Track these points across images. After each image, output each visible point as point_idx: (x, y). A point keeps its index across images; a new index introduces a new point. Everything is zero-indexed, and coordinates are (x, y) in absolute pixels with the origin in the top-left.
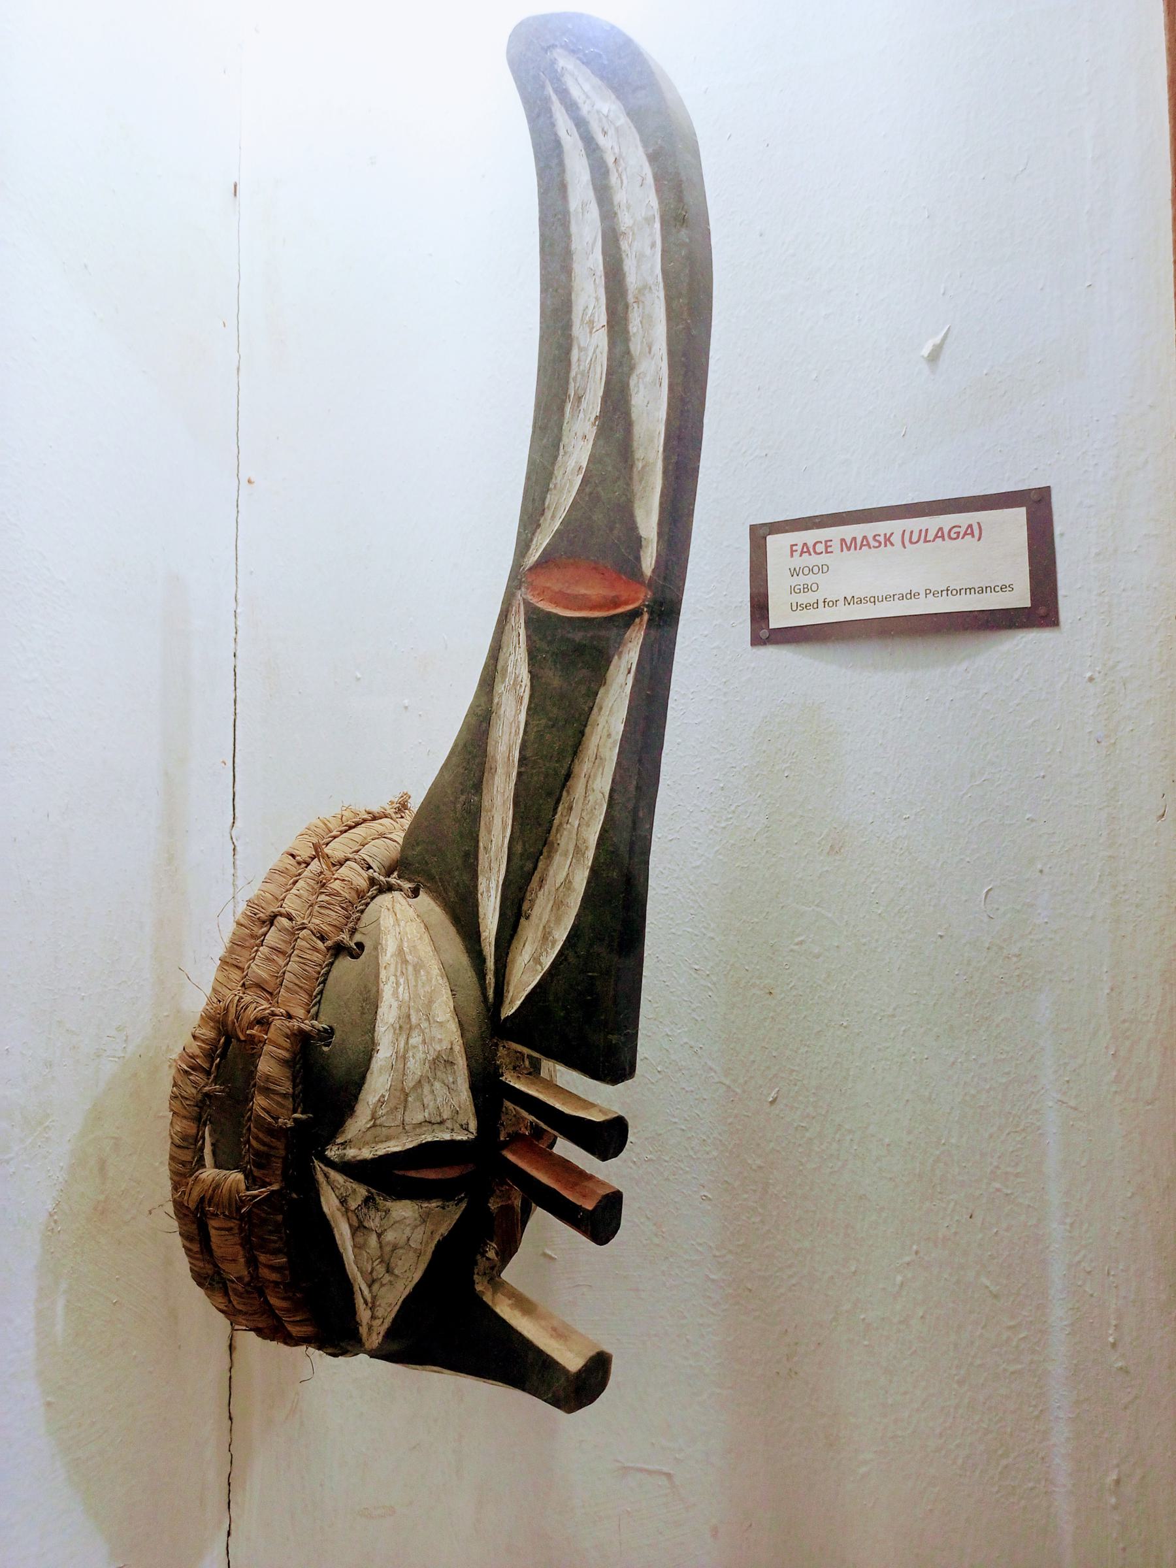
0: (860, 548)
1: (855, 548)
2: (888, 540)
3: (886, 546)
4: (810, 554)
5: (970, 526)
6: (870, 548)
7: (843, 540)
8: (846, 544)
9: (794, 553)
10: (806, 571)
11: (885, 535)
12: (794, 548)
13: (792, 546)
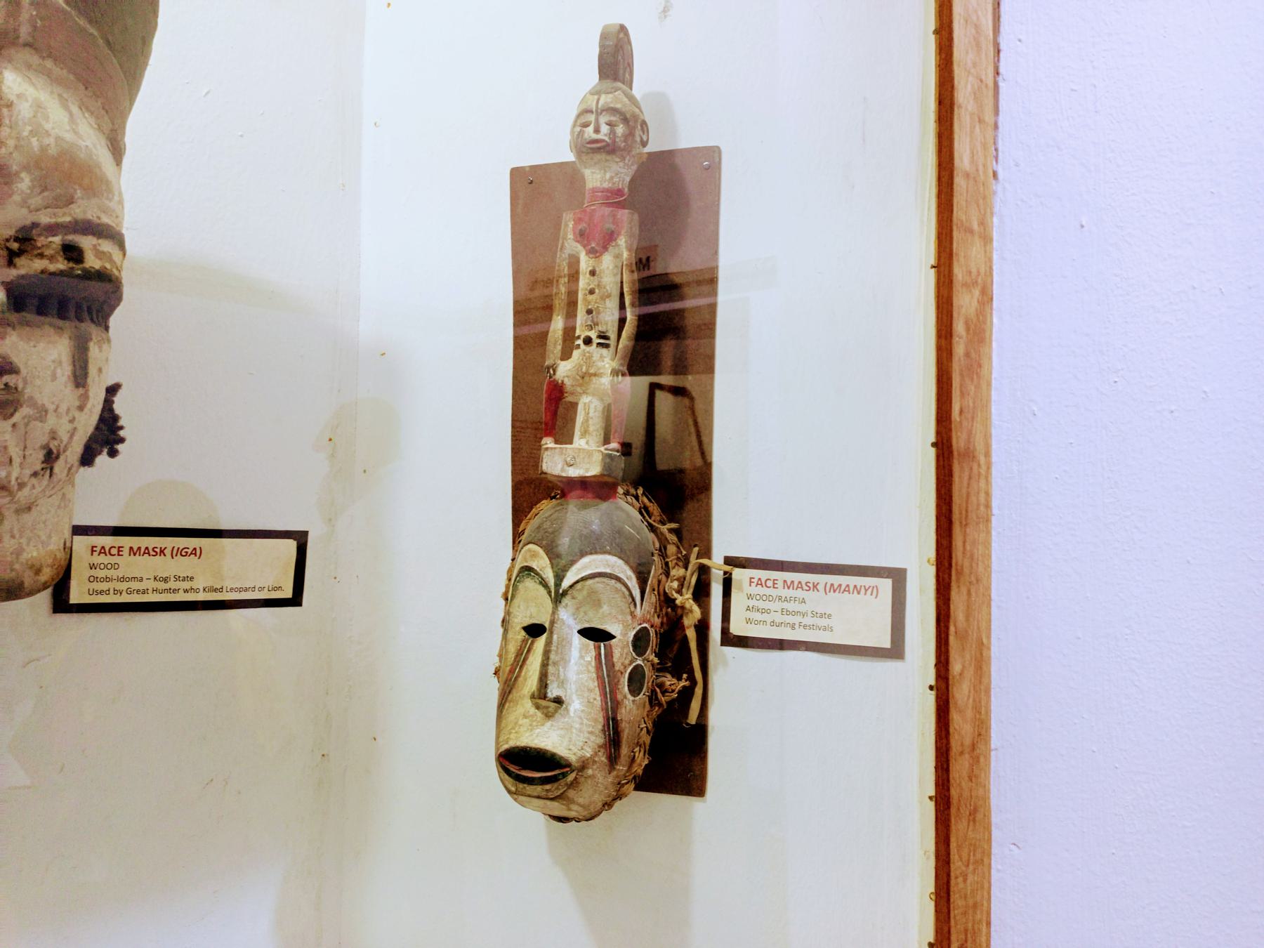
2: (162, 552)
4: (106, 555)
5: (195, 549)
7: (131, 548)
9: (94, 553)
10: (102, 566)
11: (161, 548)
12: (95, 549)
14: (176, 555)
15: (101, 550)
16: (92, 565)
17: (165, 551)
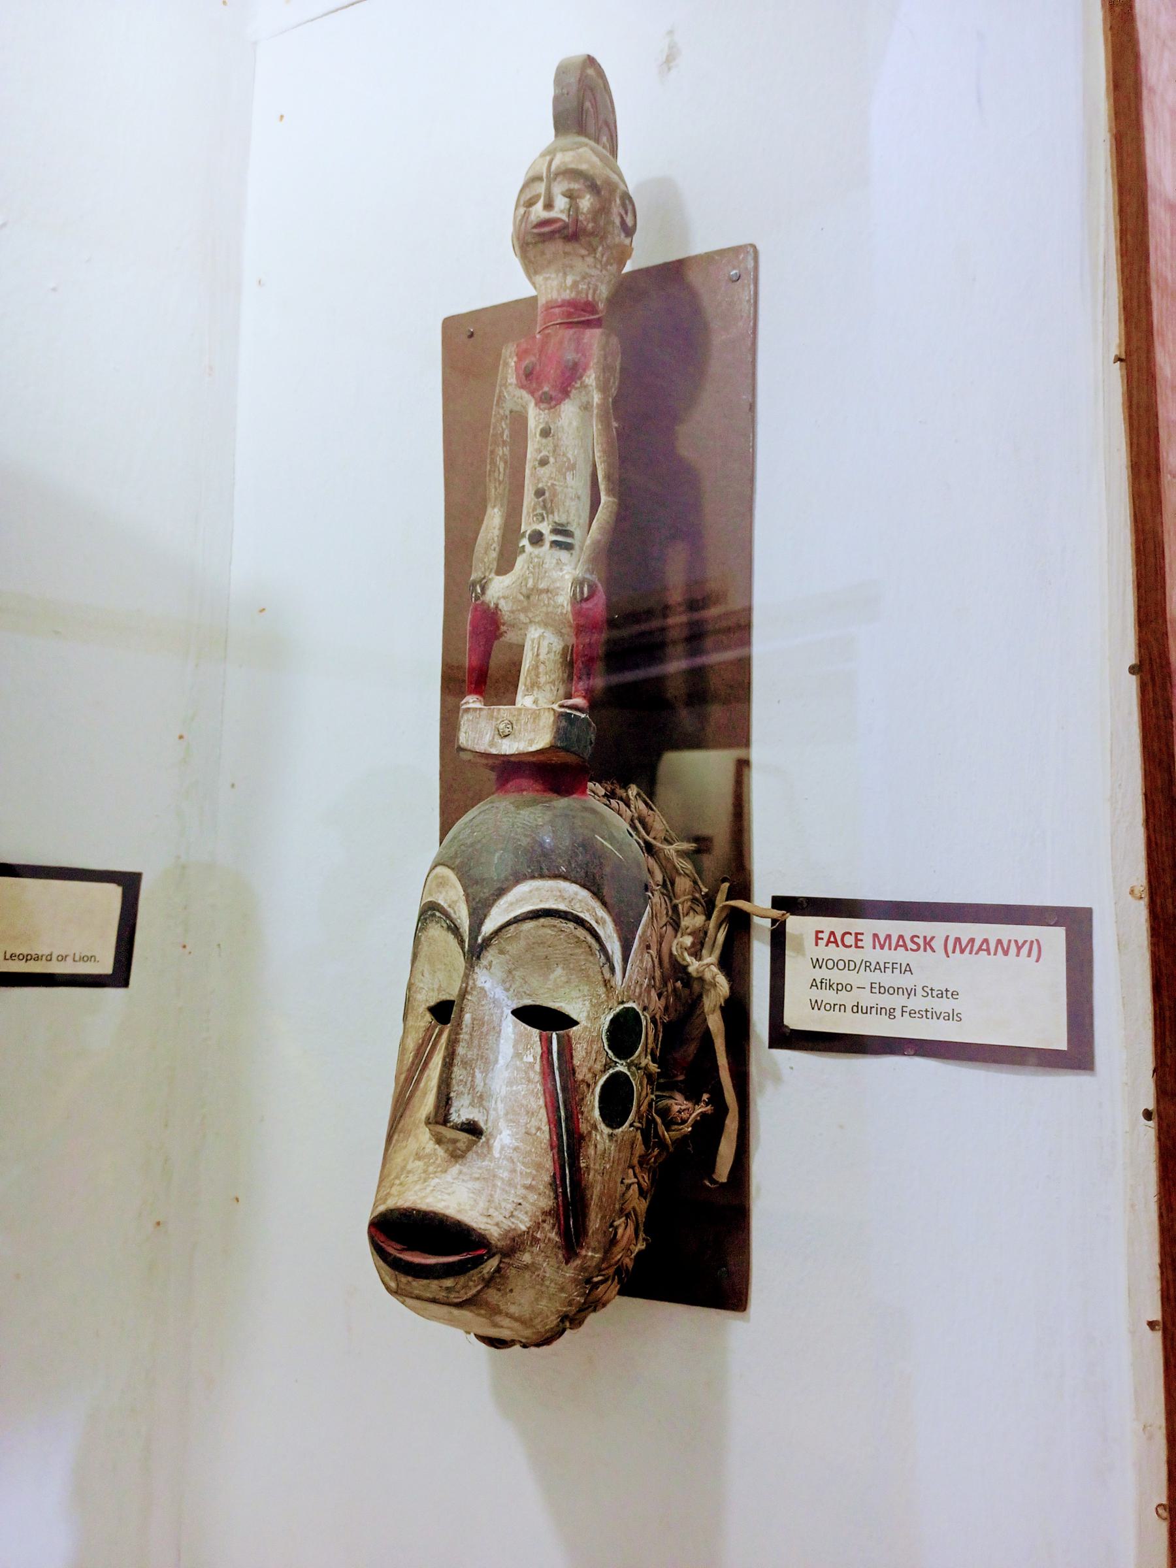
0: (895, 949)
1: (890, 949)
2: (928, 943)
3: (925, 950)
4: (838, 946)
6: (907, 950)
7: (875, 936)
8: (879, 939)
10: (830, 964)
11: (925, 938)
12: (820, 935)
13: (817, 932)
14: (954, 952)
15: (830, 937)
16: (815, 961)
17: (933, 944)
